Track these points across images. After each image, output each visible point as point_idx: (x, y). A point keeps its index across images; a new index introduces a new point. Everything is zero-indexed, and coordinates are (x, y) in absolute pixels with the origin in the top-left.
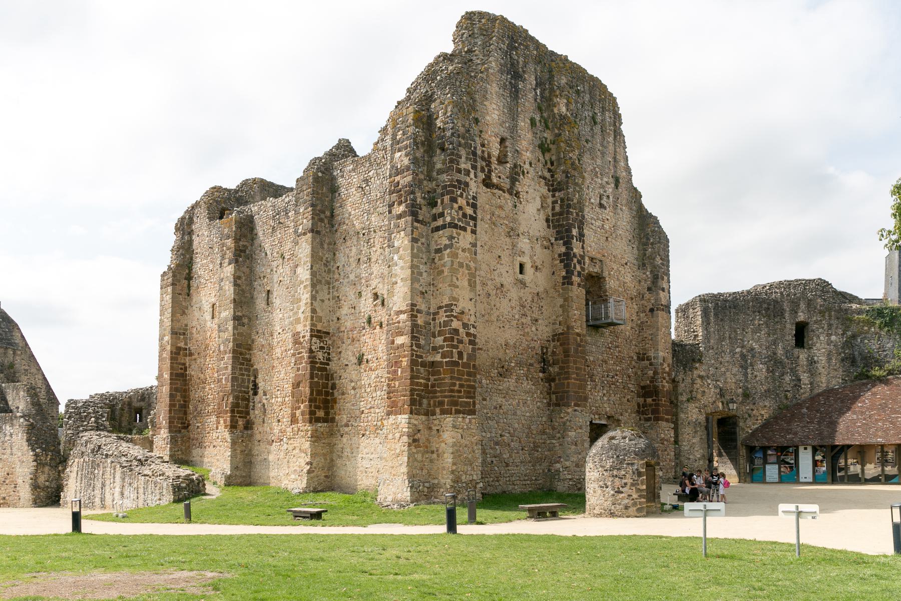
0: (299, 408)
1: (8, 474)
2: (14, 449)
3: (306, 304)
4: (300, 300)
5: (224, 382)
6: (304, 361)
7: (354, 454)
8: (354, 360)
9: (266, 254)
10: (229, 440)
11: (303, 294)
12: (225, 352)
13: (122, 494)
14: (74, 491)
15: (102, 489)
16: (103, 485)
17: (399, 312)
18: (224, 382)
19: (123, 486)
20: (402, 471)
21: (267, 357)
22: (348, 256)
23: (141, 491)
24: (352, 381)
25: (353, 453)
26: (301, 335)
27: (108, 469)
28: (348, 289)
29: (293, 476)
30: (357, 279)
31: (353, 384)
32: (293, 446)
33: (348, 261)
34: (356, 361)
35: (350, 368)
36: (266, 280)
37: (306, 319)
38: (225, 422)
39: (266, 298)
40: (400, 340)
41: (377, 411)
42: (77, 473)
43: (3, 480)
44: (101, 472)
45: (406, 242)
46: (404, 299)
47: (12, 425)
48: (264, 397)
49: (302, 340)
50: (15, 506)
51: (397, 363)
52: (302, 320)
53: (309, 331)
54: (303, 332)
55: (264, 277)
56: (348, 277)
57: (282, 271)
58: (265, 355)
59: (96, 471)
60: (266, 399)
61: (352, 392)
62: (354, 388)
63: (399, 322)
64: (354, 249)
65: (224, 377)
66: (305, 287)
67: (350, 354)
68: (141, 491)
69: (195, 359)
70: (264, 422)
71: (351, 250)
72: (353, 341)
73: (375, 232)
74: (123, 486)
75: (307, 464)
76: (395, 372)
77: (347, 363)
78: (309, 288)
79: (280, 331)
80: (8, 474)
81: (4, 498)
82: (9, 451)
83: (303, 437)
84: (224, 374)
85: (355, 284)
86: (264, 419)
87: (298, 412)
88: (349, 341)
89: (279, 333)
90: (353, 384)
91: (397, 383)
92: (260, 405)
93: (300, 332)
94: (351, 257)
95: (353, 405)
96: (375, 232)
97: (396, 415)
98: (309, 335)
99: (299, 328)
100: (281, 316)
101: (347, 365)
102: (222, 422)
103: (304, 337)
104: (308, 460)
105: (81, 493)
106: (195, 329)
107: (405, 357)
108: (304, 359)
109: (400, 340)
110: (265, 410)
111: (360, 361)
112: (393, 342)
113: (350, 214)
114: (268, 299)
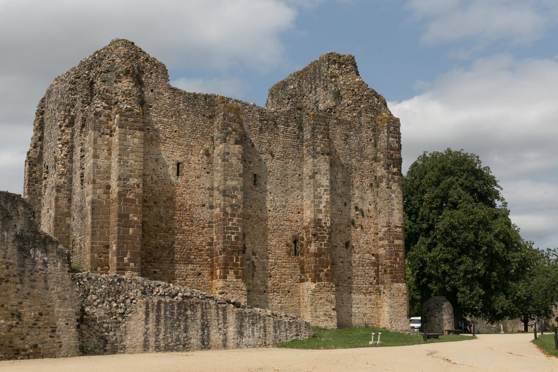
0: (323, 271)
1: (41, 314)
2: (51, 285)
3: (327, 202)
4: (321, 198)
5: (233, 240)
6: (326, 240)
7: (344, 304)
8: (341, 244)
9: (253, 145)
10: (244, 289)
11: (323, 194)
12: (234, 215)
13: (241, 333)
14: (140, 334)
15: (203, 330)
16: (205, 327)
17: (396, 227)
18: (233, 240)
19: (241, 326)
20: (404, 314)
21: (256, 226)
22: (335, 177)
23: (270, 329)
24: (340, 257)
25: (343, 303)
26: (323, 221)
27: (213, 311)
28: (336, 198)
29: (323, 318)
30: (343, 194)
31: (342, 260)
32: (320, 297)
33: (336, 180)
34: (344, 245)
35: (338, 249)
36: (252, 165)
37: (326, 211)
38: (236, 273)
39: (253, 179)
40: (397, 242)
41: (360, 278)
42: (147, 314)
43: (33, 321)
44: (199, 314)
45: (399, 190)
46: (399, 219)
47: (46, 251)
48: (253, 257)
49: (324, 225)
50: (53, 355)
51: (397, 255)
52: (323, 211)
53: (330, 220)
54: (324, 220)
55: (250, 162)
56: (336, 190)
57: (272, 164)
58: (253, 223)
59: (189, 312)
60: (256, 258)
61: (341, 264)
62: (342, 262)
63: (396, 232)
64: (340, 175)
65: (233, 236)
66: (325, 190)
67: (339, 240)
68: (270, 329)
69: (148, 207)
70: (253, 276)
71: (337, 174)
72: (340, 232)
73: (356, 170)
74: (241, 326)
75: (334, 309)
76: (396, 259)
77: (336, 245)
78: (329, 192)
79: (271, 209)
80: (41, 314)
81: (35, 346)
82: (42, 284)
83: (328, 291)
84: (233, 233)
85: (341, 197)
86: (253, 274)
87: (322, 274)
88: (337, 232)
89: (269, 211)
90: (342, 260)
91: (397, 266)
92: (248, 262)
93: (321, 219)
94: (338, 178)
95: (342, 273)
96: (356, 170)
97: (397, 283)
98: (330, 223)
99: (321, 216)
100: (271, 198)
101: (336, 246)
102: (231, 272)
103: (325, 223)
104: (334, 307)
105: (158, 335)
106: (150, 178)
107: (401, 252)
108: (326, 238)
109: (397, 242)
110: (254, 267)
111: (347, 245)
112: (393, 242)
113: (336, 151)
114: (255, 181)
